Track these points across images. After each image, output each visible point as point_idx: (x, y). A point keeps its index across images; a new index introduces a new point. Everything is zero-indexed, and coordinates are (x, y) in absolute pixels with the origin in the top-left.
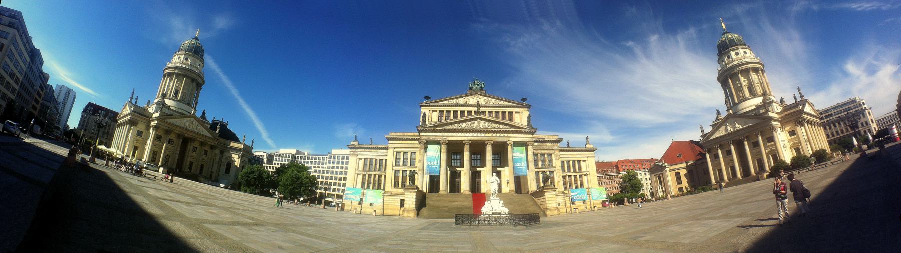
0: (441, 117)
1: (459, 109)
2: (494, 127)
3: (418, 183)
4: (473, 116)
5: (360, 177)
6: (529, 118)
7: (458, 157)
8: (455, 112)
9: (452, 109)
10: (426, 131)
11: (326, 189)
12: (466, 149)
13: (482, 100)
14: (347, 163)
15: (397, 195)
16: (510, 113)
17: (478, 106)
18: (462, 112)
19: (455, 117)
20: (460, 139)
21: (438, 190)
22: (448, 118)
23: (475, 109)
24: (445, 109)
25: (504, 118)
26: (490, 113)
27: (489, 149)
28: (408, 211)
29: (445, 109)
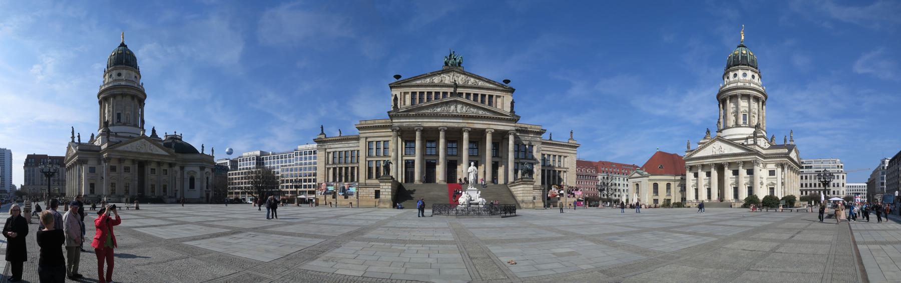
0: (413, 99)
1: (433, 90)
2: (473, 111)
3: (392, 173)
4: (449, 98)
5: (331, 171)
6: (512, 103)
7: (433, 145)
8: (429, 93)
9: (425, 90)
10: (398, 117)
11: (296, 187)
12: (442, 134)
13: (460, 79)
14: (315, 158)
15: (372, 186)
16: (491, 97)
17: (456, 86)
18: (437, 93)
19: (429, 99)
20: (435, 125)
21: (412, 180)
22: (421, 100)
23: (452, 90)
24: (418, 90)
25: (483, 102)
26: (468, 95)
27: (466, 136)
28: (384, 202)
29: (418, 90)
